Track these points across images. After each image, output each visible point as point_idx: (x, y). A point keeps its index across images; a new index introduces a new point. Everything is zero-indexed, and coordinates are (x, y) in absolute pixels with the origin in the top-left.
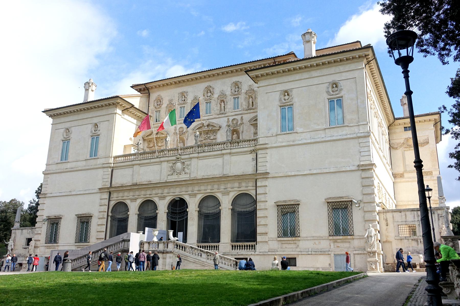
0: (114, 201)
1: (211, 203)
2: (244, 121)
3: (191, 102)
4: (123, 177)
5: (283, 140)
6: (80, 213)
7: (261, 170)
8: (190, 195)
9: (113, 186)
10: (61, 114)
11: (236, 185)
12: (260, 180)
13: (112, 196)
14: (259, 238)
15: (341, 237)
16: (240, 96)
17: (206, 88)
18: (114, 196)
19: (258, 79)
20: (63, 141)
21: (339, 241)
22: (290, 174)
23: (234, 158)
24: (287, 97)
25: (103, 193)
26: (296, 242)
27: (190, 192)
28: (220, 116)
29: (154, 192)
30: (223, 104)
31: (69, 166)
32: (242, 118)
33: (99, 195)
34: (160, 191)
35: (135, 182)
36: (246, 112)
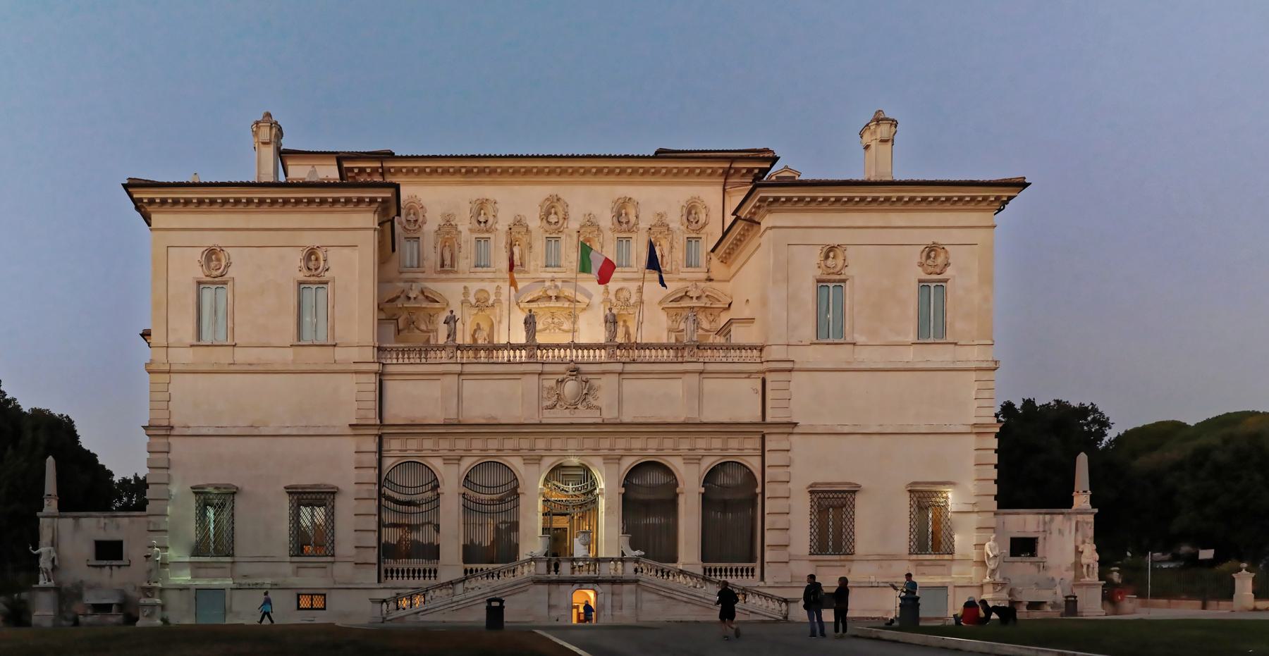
0: (393, 460)
1: (654, 478)
6: (293, 483)
9: (386, 422)
13: (385, 447)
16: (634, 236)
18: (393, 445)
22: (839, 430)
32: (640, 290)
34: (525, 443)
35: (452, 415)
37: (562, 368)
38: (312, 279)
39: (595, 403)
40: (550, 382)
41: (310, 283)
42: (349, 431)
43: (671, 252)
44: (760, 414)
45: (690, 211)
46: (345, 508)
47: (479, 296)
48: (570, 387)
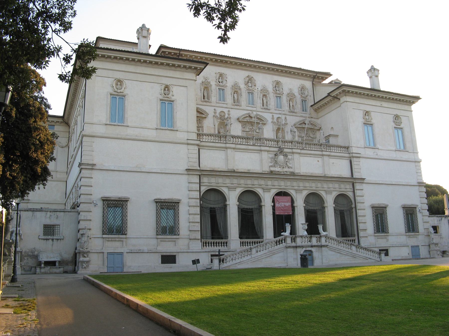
2: (288, 122)
3: (231, 86)
4: (213, 159)
5: (370, 153)
7: (356, 175)
8: (296, 190)
10: (109, 57)
11: (337, 186)
12: (357, 184)
14: (361, 234)
15: (413, 234)
17: (248, 77)
19: (347, 94)
20: (111, 94)
21: (411, 236)
23: (332, 160)
24: (367, 117)
25: (190, 176)
26: (387, 237)
27: (296, 188)
28: (264, 110)
29: (256, 182)
30: (264, 99)
31: (130, 132)
33: (186, 177)
34: (262, 182)
35: (231, 167)
36: (289, 114)
37: (276, 149)
38: (166, 99)
39: (290, 166)
40: (272, 155)
41: (165, 100)
42: (186, 173)
43: (296, 104)
44: (350, 174)
45: (302, 89)
46: (183, 210)
47: (223, 114)
48: (281, 158)
